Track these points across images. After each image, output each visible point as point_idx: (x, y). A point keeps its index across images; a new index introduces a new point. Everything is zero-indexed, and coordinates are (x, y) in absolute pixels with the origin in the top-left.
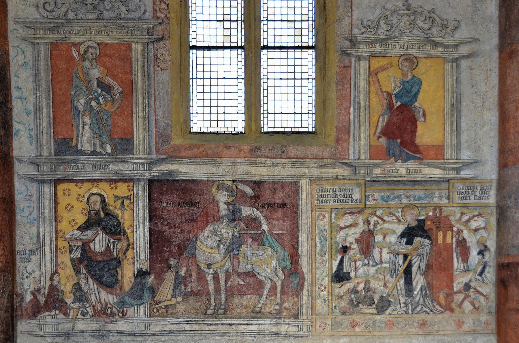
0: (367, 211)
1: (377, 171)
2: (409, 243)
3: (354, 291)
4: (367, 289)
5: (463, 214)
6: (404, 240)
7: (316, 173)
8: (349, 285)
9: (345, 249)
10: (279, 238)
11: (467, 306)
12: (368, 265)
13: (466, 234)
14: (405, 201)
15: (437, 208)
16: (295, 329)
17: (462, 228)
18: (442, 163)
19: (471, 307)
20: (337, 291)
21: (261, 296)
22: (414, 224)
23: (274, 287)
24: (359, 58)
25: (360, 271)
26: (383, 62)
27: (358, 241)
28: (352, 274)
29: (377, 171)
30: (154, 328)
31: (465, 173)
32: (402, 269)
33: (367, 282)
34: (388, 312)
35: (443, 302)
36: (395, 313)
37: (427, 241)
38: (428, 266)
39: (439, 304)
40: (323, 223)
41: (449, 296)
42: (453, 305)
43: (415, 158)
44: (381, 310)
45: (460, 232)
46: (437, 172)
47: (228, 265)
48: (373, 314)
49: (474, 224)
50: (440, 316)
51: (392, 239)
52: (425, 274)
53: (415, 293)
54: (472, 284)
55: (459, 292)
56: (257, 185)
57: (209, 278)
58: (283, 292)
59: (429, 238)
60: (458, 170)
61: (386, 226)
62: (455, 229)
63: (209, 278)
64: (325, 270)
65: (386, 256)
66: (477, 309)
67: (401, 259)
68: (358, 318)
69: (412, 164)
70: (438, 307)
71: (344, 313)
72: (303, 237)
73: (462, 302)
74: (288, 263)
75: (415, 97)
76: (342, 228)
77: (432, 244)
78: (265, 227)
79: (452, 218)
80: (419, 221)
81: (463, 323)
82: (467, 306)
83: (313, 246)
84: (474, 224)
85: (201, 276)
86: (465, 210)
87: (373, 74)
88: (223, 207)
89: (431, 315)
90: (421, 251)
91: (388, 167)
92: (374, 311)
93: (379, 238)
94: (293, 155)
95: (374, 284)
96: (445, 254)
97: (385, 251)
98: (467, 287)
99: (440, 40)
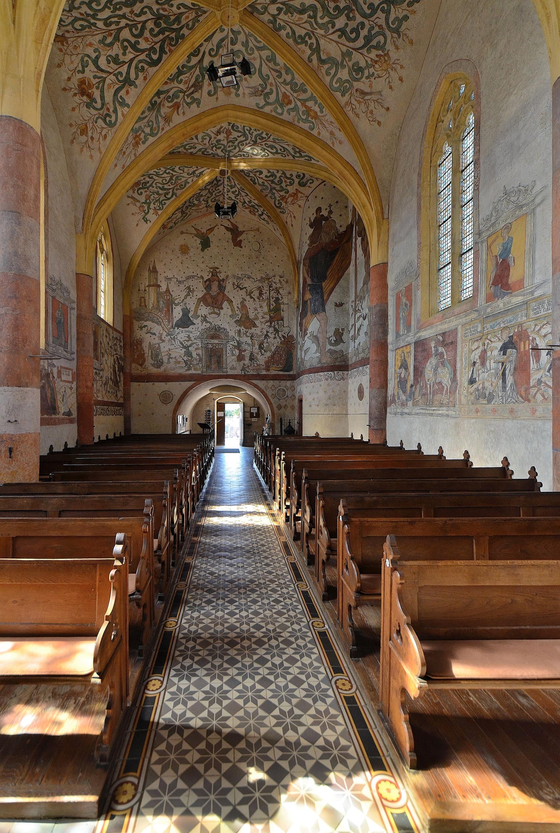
0: (484, 337)
1: (489, 310)
2: (504, 354)
3: (477, 390)
4: (483, 388)
5: (536, 325)
6: (502, 353)
7: (464, 320)
8: (475, 386)
9: (474, 363)
10: (449, 361)
11: (539, 397)
12: (484, 372)
13: (538, 341)
14: (502, 325)
15: (520, 325)
16: (454, 413)
17: (535, 336)
18: (522, 292)
19: (542, 398)
20: (470, 390)
21: (443, 394)
22: (507, 340)
23: (447, 389)
24: (482, 242)
25: (481, 377)
26: (494, 237)
27: (480, 357)
28: (477, 379)
29: (489, 310)
30: (414, 411)
31: (537, 294)
32: (501, 373)
33: (483, 383)
34: (493, 402)
35: (524, 395)
36: (496, 403)
37: (514, 350)
38: (515, 369)
39: (521, 397)
40: (466, 349)
41: (527, 390)
42: (530, 397)
43: (508, 294)
44: (489, 402)
45: (534, 339)
46: (520, 299)
47: (434, 379)
48: (485, 404)
49: (543, 332)
50: (522, 405)
51: (496, 352)
52: (513, 375)
53: (507, 389)
54: (543, 379)
55: (534, 386)
56: (443, 334)
57: (428, 386)
58: (450, 393)
59: (516, 349)
60: (532, 293)
61: (493, 345)
62: (531, 338)
63: (428, 386)
64: (466, 378)
65: (493, 365)
66: (546, 399)
67: (500, 364)
68: (478, 406)
69: (506, 299)
70: (520, 398)
71: (473, 404)
72: (458, 359)
73: (536, 394)
74: (452, 376)
75: (510, 251)
76: (473, 351)
77: (517, 352)
78: (445, 357)
79: (529, 331)
80: (510, 337)
81: (536, 410)
82: (539, 397)
83: (462, 364)
84: (543, 332)
85: (426, 387)
86: (537, 322)
87: (489, 248)
88: (433, 349)
89: (517, 404)
90: (511, 358)
91: (494, 305)
92: (485, 402)
93: (489, 353)
94: (456, 313)
95: (487, 384)
96: (525, 358)
97: (492, 361)
98: (539, 381)
99: (524, 202)
